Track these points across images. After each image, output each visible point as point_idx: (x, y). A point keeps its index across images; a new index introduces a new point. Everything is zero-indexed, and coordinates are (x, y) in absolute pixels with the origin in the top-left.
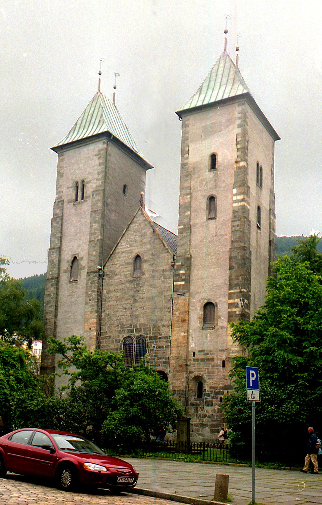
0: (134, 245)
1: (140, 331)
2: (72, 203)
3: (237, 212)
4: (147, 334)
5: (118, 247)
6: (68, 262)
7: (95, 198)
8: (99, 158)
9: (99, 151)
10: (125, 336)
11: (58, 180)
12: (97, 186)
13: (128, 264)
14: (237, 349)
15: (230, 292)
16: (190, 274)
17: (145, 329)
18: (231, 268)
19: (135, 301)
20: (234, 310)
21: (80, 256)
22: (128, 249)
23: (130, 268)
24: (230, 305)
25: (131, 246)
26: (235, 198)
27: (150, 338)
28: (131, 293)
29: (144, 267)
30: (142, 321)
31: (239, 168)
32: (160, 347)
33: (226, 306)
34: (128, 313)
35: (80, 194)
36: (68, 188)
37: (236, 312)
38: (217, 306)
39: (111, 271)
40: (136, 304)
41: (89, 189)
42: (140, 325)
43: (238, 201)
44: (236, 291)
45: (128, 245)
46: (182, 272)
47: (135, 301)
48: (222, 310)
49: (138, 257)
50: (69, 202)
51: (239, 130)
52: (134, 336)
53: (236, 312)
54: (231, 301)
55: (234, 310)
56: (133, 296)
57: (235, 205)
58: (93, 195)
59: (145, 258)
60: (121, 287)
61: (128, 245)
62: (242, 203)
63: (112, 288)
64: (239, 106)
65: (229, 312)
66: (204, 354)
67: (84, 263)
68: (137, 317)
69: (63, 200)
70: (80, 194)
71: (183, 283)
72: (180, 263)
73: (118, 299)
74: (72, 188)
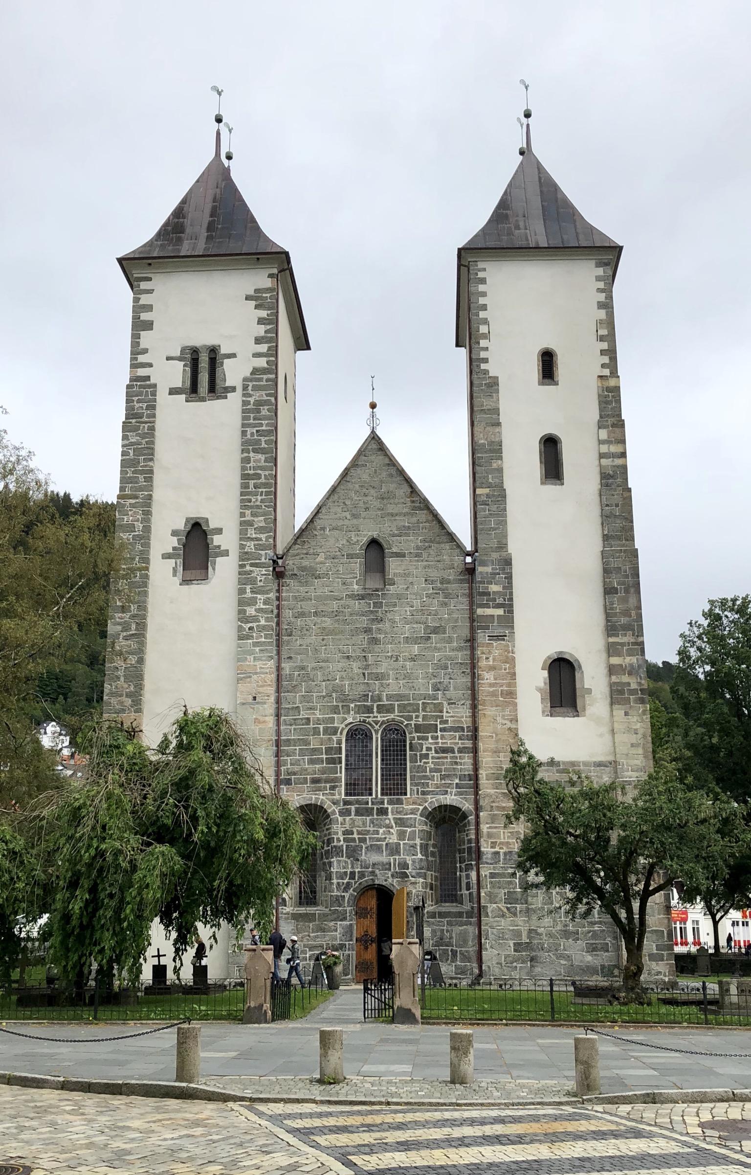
0: (363, 514)
1: (389, 709)
2: (183, 396)
3: (612, 477)
4: (410, 718)
5: (320, 516)
6: (175, 533)
7: (250, 396)
8: (256, 307)
9: (256, 291)
10: (350, 720)
11: (136, 337)
12: (255, 371)
13: (350, 556)
14: (638, 762)
15: (611, 640)
16: (511, 594)
17: (402, 708)
18: (609, 591)
19: (375, 641)
20: (625, 679)
21: (213, 525)
22: (346, 522)
23: (357, 565)
24: (612, 670)
25: (355, 516)
26: (604, 449)
27: (418, 728)
28: (364, 622)
29: (392, 566)
30: (394, 686)
31: (609, 389)
32: (445, 750)
33: (603, 671)
34: (356, 666)
35: (204, 378)
36: (168, 359)
37: (629, 684)
38: (580, 667)
39: (303, 569)
40: (377, 648)
41: (234, 373)
42: (389, 697)
43: (613, 456)
44: (625, 640)
45: (348, 515)
46: (494, 588)
47: (375, 641)
48: (593, 677)
49: (374, 544)
50: (173, 391)
51: (602, 314)
52: (376, 723)
53: (629, 684)
54: (615, 660)
55: (625, 679)
56: (367, 631)
57: (604, 461)
58: (245, 388)
59: (394, 550)
60: (335, 605)
61: (348, 515)
62: (619, 462)
63: (309, 607)
64: (598, 265)
65: (611, 685)
66: (558, 771)
67: (227, 540)
68: (379, 677)
69: (155, 386)
70: (204, 378)
71: (500, 612)
72: (489, 569)
73: (325, 632)
74: (180, 359)
